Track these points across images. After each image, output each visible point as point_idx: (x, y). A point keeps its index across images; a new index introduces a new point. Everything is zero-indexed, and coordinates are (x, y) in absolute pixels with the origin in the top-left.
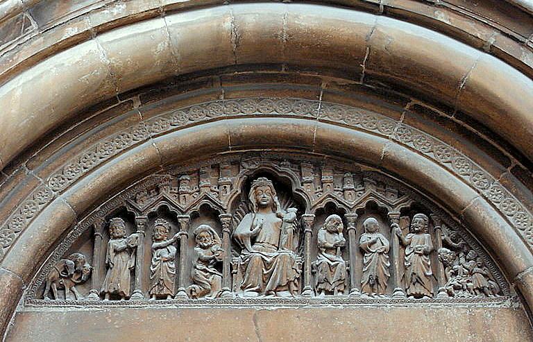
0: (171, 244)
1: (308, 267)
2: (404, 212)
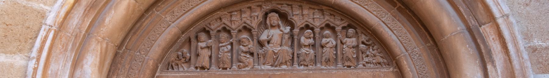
0: (228, 44)
1: (295, 55)
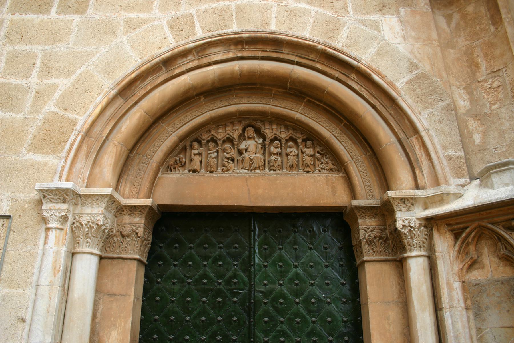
0: (215, 152)
1: (267, 161)
2: (303, 140)
